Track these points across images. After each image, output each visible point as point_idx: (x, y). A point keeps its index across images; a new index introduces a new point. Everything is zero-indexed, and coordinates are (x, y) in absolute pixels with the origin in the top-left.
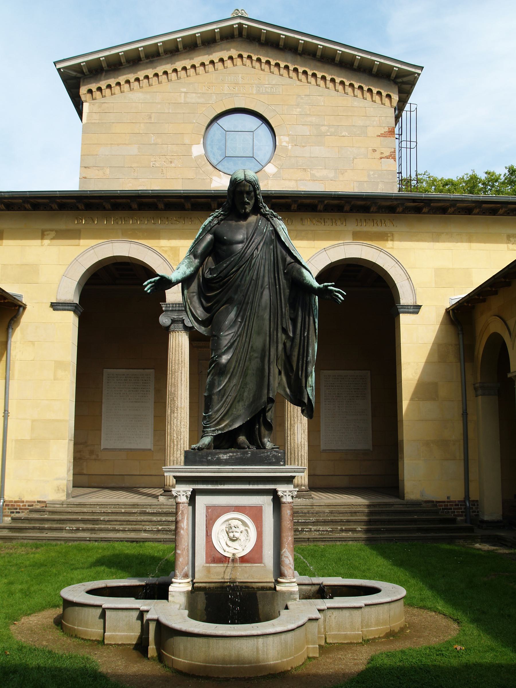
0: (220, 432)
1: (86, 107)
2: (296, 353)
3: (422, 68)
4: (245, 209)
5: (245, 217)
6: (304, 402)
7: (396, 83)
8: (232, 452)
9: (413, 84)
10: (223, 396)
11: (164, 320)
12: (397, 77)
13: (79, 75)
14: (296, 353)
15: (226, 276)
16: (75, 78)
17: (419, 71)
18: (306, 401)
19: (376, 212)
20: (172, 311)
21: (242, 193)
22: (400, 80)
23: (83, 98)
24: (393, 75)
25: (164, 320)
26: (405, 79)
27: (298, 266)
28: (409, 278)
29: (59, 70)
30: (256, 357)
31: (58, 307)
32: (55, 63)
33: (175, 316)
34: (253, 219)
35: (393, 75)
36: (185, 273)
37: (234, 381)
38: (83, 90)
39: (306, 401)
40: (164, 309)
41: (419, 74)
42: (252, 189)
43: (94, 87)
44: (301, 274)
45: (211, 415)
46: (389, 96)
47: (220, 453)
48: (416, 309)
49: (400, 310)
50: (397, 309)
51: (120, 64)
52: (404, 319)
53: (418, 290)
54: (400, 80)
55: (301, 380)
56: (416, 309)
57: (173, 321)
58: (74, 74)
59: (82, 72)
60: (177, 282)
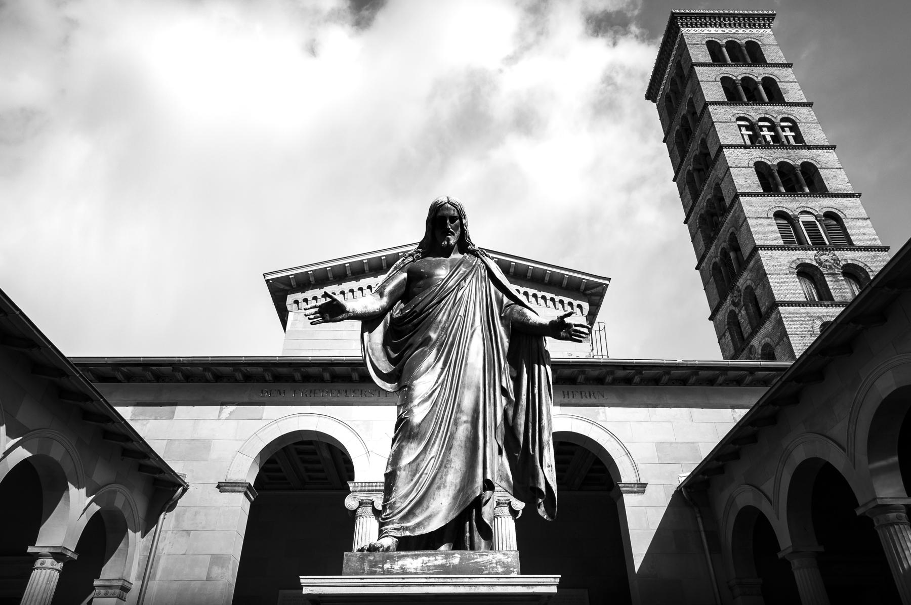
0: (408, 533)
1: (291, 316)
2: (521, 421)
3: (609, 279)
4: (449, 240)
5: (447, 252)
6: (541, 491)
7: (585, 295)
8: (428, 555)
9: (602, 295)
10: (414, 475)
11: (351, 502)
12: (587, 289)
13: (287, 288)
14: (521, 421)
15: (422, 312)
16: (283, 290)
17: (607, 282)
18: (543, 487)
19: (583, 384)
20: (361, 491)
21: (443, 219)
22: (589, 292)
23: (289, 308)
24: (583, 287)
25: (351, 502)
26: (593, 291)
27: (520, 307)
28: (628, 453)
29: (267, 281)
30: (465, 422)
31: (227, 488)
32: (264, 275)
33: (363, 497)
34: (456, 256)
35: (583, 287)
36: (366, 307)
37: (434, 451)
38: (290, 299)
39: (543, 487)
40: (351, 489)
41: (607, 285)
42: (456, 214)
43: (299, 296)
44: (524, 315)
45: (394, 503)
46: (579, 306)
47: (407, 556)
48: (641, 488)
49: (623, 489)
50: (619, 488)
51: (328, 279)
52: (630, 501)
53: (641, 467)
54: (589, 292)
55: (533, 456)
56: (641, 488)
57: (361, 504)
58: (282, 286)
59: (290, 285)
60: (356, 317)
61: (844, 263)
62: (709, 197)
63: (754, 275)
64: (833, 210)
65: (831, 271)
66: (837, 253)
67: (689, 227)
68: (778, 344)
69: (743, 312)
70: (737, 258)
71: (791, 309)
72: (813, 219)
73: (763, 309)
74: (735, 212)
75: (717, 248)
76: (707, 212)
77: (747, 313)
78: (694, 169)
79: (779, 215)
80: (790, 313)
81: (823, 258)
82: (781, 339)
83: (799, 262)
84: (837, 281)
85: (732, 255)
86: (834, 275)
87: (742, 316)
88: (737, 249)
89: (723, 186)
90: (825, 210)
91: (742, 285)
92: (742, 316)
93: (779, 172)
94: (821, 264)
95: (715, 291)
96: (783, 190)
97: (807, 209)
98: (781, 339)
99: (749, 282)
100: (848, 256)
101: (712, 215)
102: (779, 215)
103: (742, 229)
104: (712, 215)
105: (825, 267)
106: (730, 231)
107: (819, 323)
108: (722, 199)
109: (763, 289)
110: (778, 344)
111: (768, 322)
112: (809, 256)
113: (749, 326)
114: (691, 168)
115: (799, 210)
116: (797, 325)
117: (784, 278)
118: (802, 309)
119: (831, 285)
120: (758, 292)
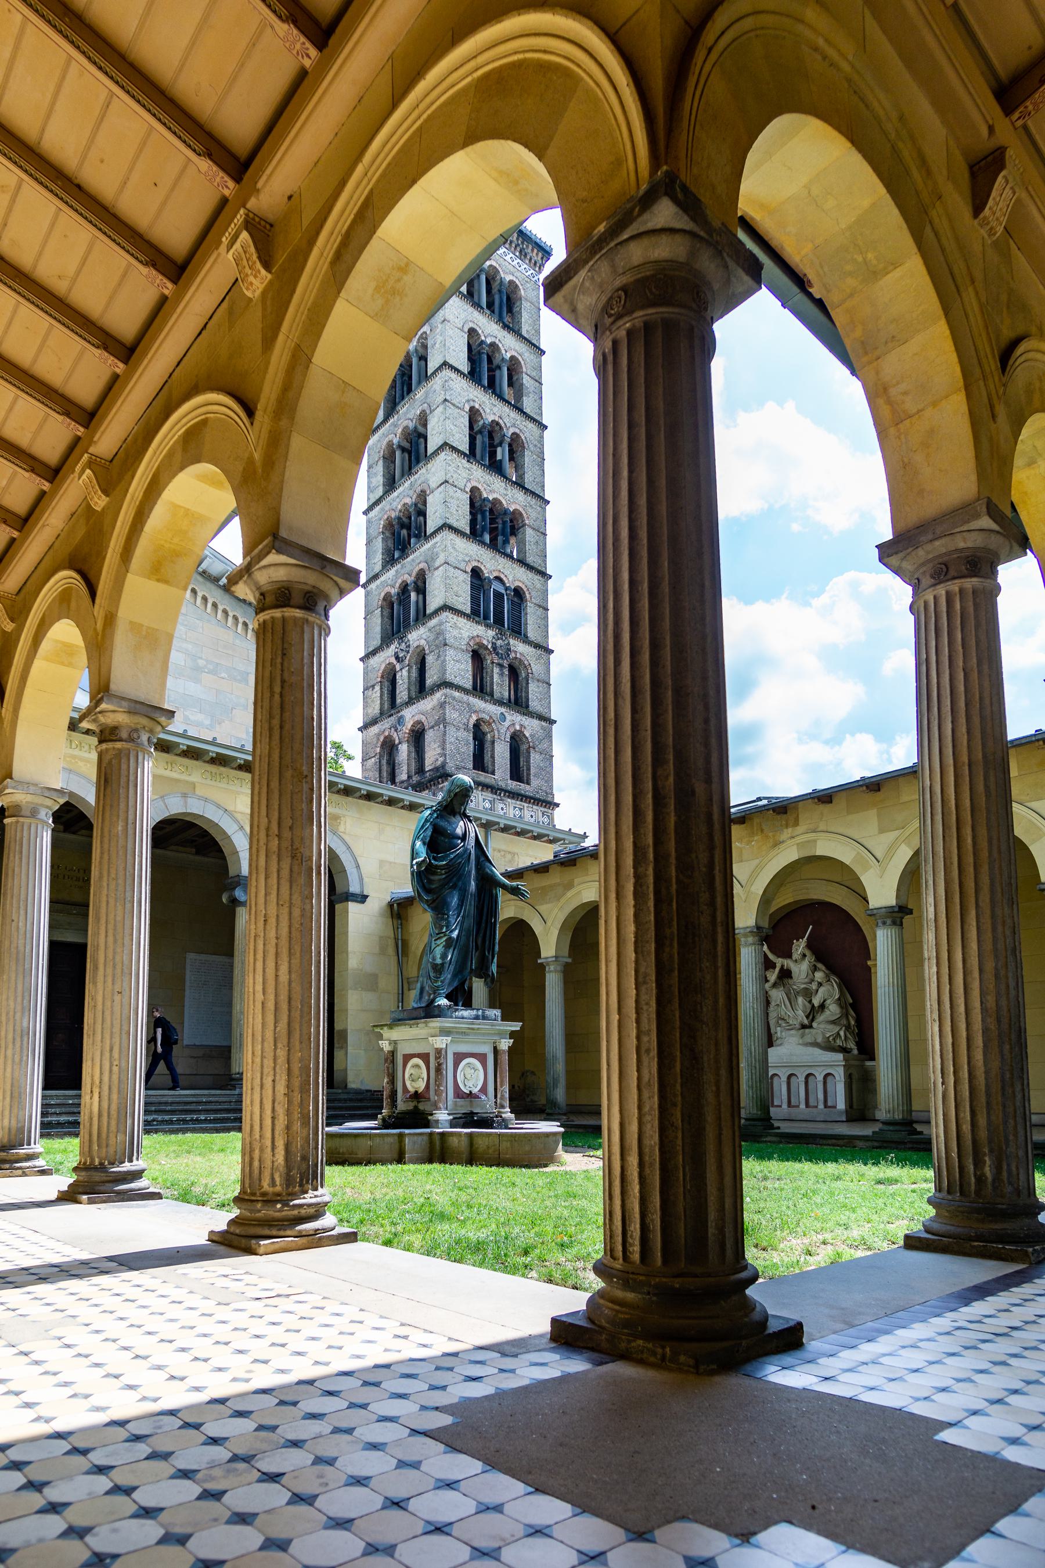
61: (513, 655)
62: (408, 501)
63: (432, 638)
64: (523, 587)
65: (501, 661)
66: (512, 641)
67: (369, 522)
68: (432, 727)
69: (405, 672)
70: (417, 602)
71: (457, 694)
72: (503, 591)
73: (429, 682)
74: (434, 546)
75: (397, 575)
76: (399, 518)
77: (409, 677)
78: (400, 447)
79: (476, 573)
80: (454, 698)
81: (499, 643)
82: (437, 724)
83: (477, 640)
84: (502, 674)
85: (413, 596)
86: (501, 666)
87: (404, 678)
88: (422, 591)
89: (430, 499)
90: (517, 584)
91: (414, 641)
92: (404, 678)
93: (491, 511)
94: (495, 648)
95: (378, 629)
96: (487, 538)
97: (502, 576)
98: (437, 724)
99: (423, 642)
100: (520, 648)
101: (402, 526)
102: (476, 573)
103: (436, 573)
104: (402, 526)
105: (497, 654)
106: (421, 566)
107: (474, 718)
108: (422, 513)
109: (437, 660)
110: (432, 727)
111: (429, 699)
112: (487, 635)
113: (406, 693)
114: (395, 441)
115: (495, 574)
116: (455, 715)
117: (460, 655)
118: (465, 697)
119: (496, 677)
120: (430, 659)
